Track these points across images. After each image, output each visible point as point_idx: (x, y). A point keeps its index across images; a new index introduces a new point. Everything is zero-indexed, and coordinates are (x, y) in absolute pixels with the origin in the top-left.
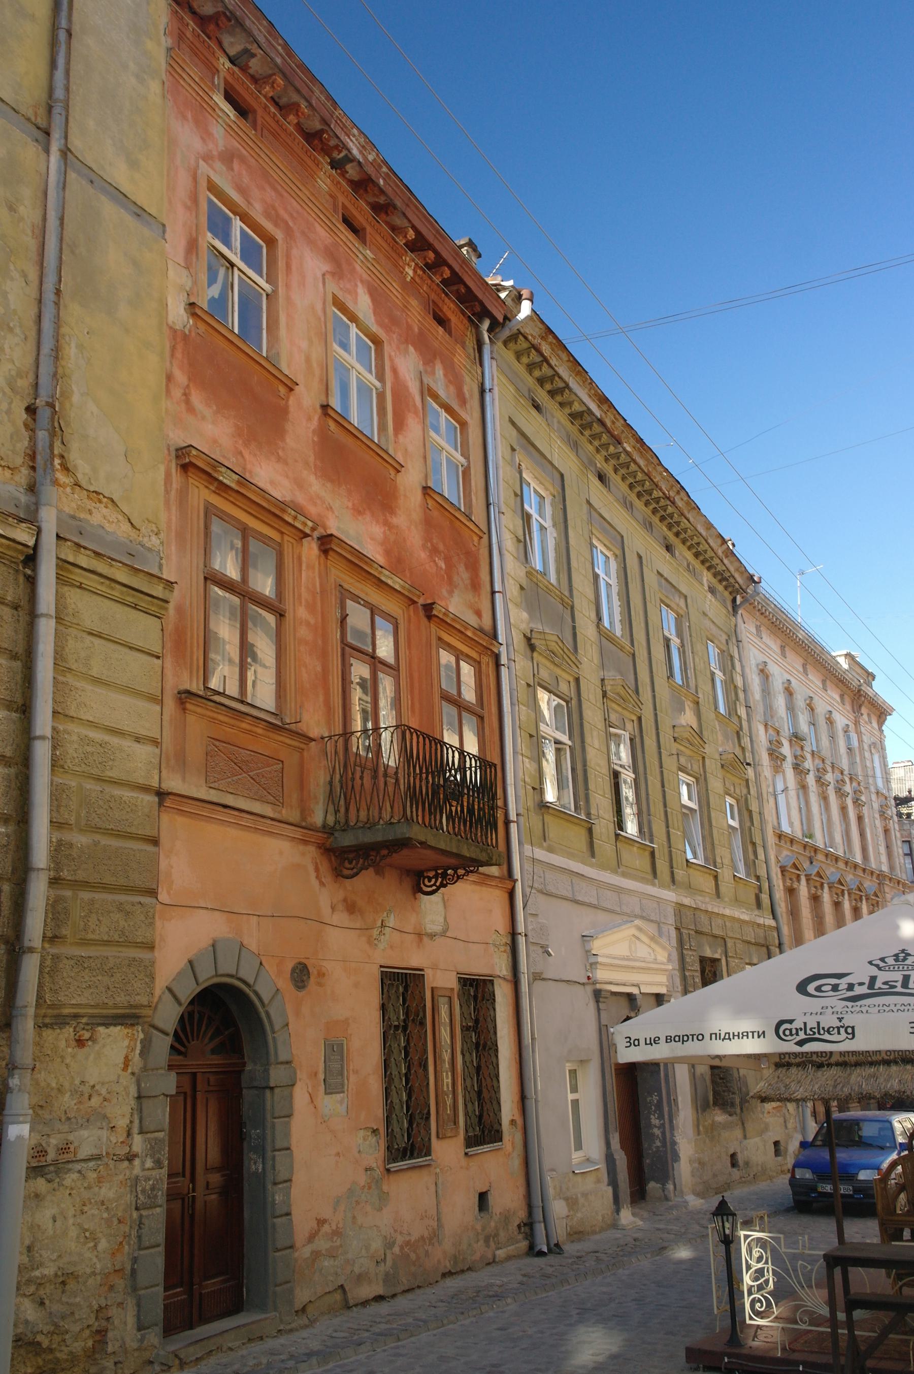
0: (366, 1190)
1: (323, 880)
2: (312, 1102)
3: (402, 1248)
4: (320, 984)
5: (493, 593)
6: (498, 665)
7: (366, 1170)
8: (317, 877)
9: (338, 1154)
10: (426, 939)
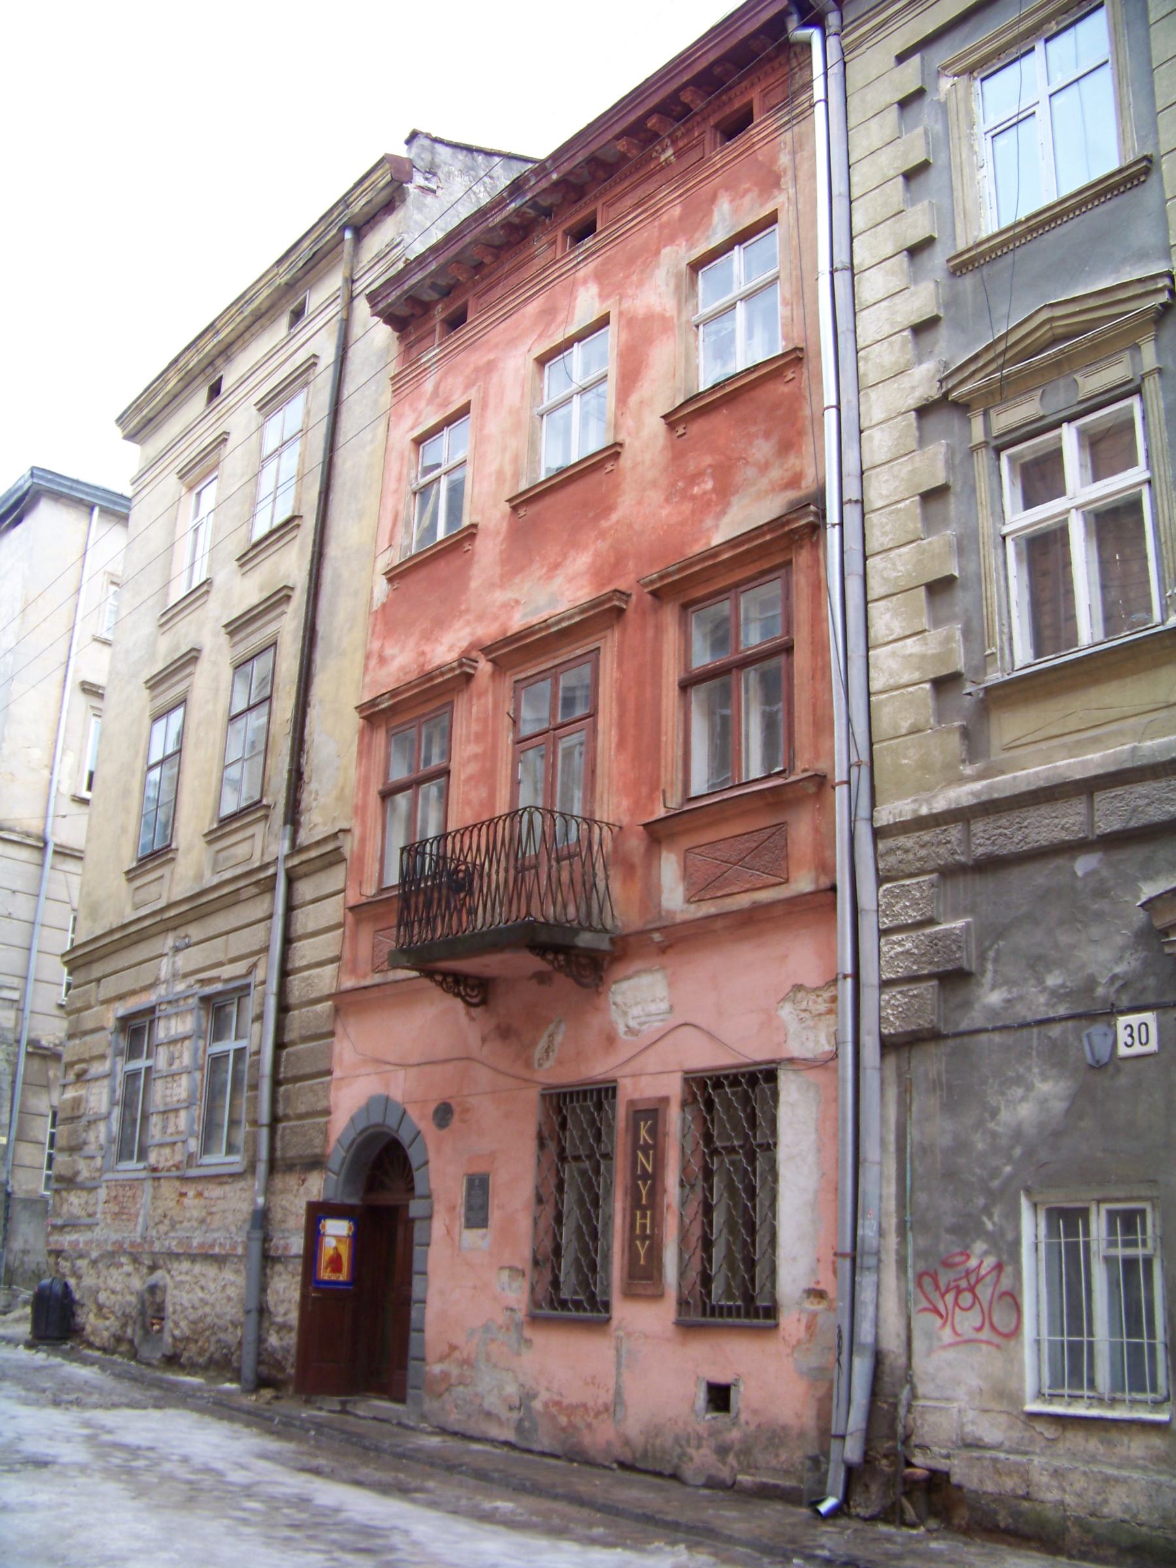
3: (546, 1405)
4: (463, 1121)
9: (475, 1287)
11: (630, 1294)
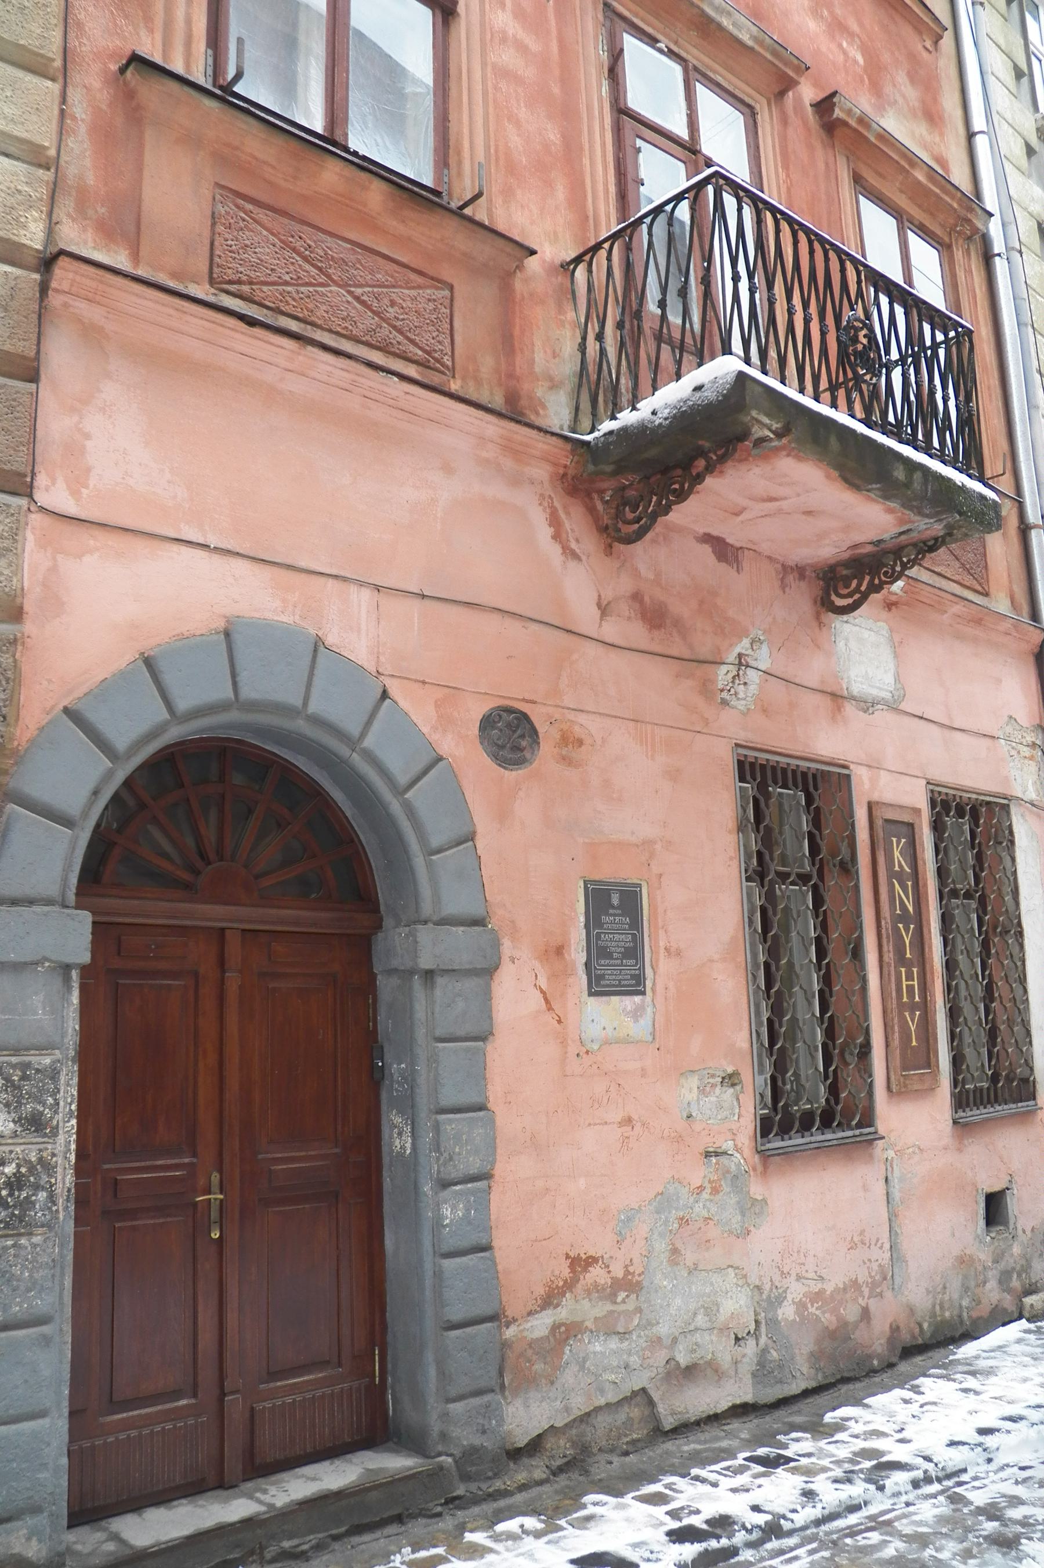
0: (705, 1195)
1: (573, 545)
2: (550, 1008)
3: (801, 1306)
4: (567, 760)
5: (970, 136)
6: (988, 258)
7: (708, 1155)
8: (557, 537)
9: (628, 1121)
10: (849, 708)
11: (896, 1092)
